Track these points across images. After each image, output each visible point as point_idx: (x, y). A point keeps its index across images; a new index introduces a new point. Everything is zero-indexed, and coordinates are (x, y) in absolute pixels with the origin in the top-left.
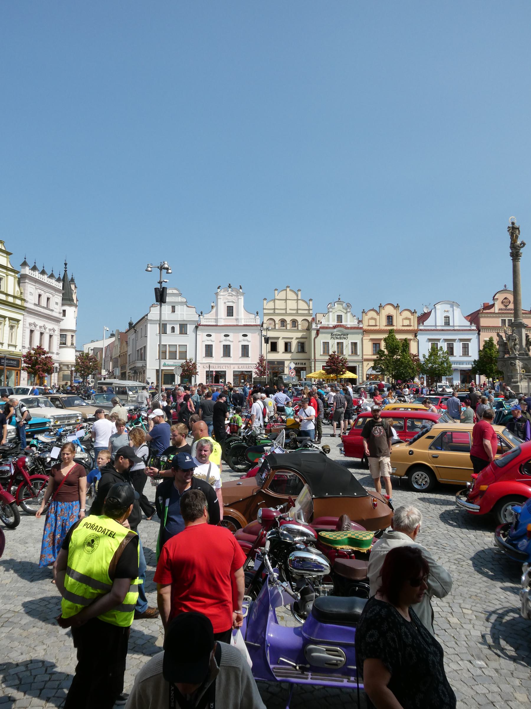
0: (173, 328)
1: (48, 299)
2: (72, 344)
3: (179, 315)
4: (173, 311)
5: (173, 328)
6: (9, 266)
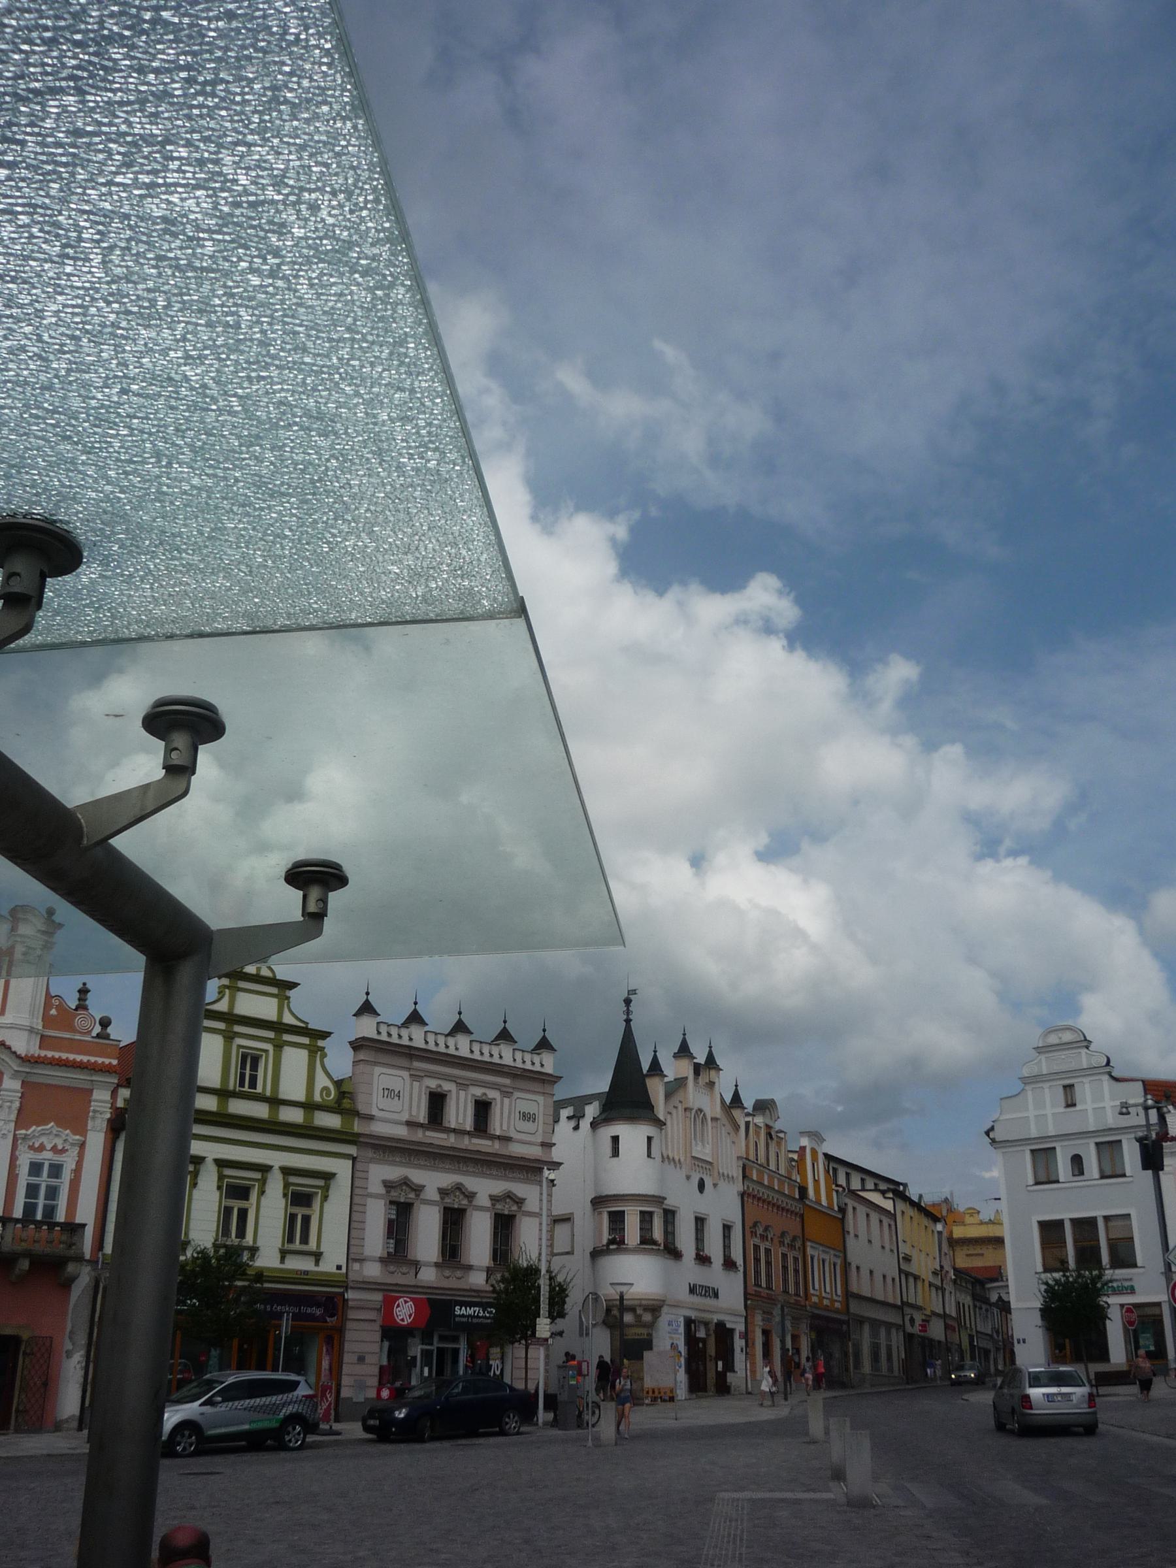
0: (1077, 1161)
1: (482, 1109)
2: (646, 1240)
3: (1090, 1112)
4: (1071, 1104)
5: (1077, 1161)
6: (288, 1019)
